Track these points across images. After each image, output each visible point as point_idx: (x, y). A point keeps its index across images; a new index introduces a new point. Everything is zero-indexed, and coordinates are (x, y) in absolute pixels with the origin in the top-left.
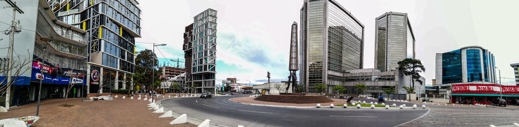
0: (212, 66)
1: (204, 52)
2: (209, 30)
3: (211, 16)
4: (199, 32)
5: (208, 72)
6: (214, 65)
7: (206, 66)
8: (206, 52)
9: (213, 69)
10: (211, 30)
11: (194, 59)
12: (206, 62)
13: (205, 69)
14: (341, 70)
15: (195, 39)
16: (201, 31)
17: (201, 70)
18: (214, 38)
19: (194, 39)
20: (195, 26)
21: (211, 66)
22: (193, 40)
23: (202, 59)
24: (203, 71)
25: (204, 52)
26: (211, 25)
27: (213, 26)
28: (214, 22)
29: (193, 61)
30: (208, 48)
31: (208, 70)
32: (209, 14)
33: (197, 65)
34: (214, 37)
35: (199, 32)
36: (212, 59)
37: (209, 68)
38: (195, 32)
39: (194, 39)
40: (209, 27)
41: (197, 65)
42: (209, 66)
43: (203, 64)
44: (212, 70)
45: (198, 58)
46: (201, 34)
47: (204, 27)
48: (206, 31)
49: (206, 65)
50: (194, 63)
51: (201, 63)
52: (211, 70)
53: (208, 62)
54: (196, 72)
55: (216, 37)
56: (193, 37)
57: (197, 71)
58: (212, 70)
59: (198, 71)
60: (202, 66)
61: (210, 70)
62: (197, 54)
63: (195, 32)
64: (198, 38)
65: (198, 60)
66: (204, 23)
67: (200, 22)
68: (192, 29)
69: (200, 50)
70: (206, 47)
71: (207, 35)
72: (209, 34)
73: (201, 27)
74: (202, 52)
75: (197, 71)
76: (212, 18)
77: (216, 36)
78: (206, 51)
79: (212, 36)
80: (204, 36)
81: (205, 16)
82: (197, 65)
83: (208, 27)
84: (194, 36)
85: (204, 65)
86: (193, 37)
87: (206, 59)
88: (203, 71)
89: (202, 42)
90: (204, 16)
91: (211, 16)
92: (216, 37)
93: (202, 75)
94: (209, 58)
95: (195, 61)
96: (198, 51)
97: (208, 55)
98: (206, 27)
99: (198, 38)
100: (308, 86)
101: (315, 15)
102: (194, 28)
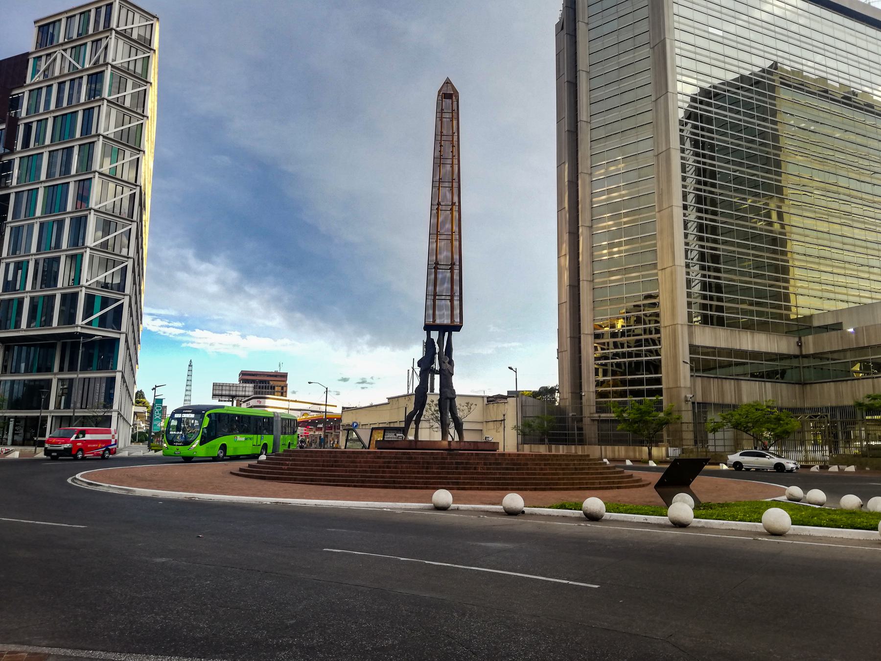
0: (105, 302)
1: (67, 223)
2: (104, 108)
3: (124, 35)
4: (52, 107)
5: (79, 330)
6: (117, 300)
7: (70, 300)
8: (79, 224)
9: (110, 319)
10: (114, 112)
11: (14, 253)
12: (77, 280)
13: (68, 317)
14: (788, 318)
15: (32, 146)
16: (65, 104)
17: (48, 322)
18: (128, 158)
19: (26, 144)
20: (35, 71)
21: (97, 303)
22: (19, 147)
23: (58, 259)
24: (55, 323)
25: (67, 223)
26: (120, 86)
27: (130, 90)
28: (139, 70)
29: (8, 265)
30: (93, 204)
31: (79, 320)
32: (114, 24)
33: (29, 291)
34: (128, 153)
35: (52, 107)
36: (110, 264)
37: (88, 312)
38: (33, 109)
39: (26, 144)
40: (105, 94)
41: (29, 287)
42: (90, 299)
43: (59, 285)
44: (103, 322)
45: (34, 249)
46: (64, 124)
47: (80, 85)
48: (88, 113)
49: (75, 295)
50: (10, 278)
51: (49, 276)
52: (97, 321)
53: (83, 282)
54: (17, 325)
55: (140, 151)
56: (21, 129)
57: (24, 325)
58: (103, 322)
59: (28, 326)
60: (54, 296)
61: (90, 323)
62: (31, 227)
63: (33, 109)
64: (48, 141)
65: (37, 263)
66: (87, 66)
67: (67, 55)
68: (21, 83)
69: (49, 208)
70: (83, 197)
71: (94, 132)
72: (101, 131)
73: (67, 85)
74: (61, 223)
75: (24, 325)
76: (127, 47)
77: (142, 148)
78: (81, 217)
79: (116, 146)
80: (78, 135)
81: (91, 31)
82: (29, 287)
83: (100, 95)
84: (28, 127)
85: (64, 296)
86: (21, 129)
87: (76, 260)
88: (56, 327)
89: (66, 171)
90: (87, 30)
91: (124, 35)
92: (140, 151)
93: (53, 346)
94: (92, 258)
95: (19, 266)
96: (38, 213)
97: (90, 241)
98: (94, 92)
99: (48, 141)
100: (594, 409)
101: (612, 39)
102: (28, 81)
